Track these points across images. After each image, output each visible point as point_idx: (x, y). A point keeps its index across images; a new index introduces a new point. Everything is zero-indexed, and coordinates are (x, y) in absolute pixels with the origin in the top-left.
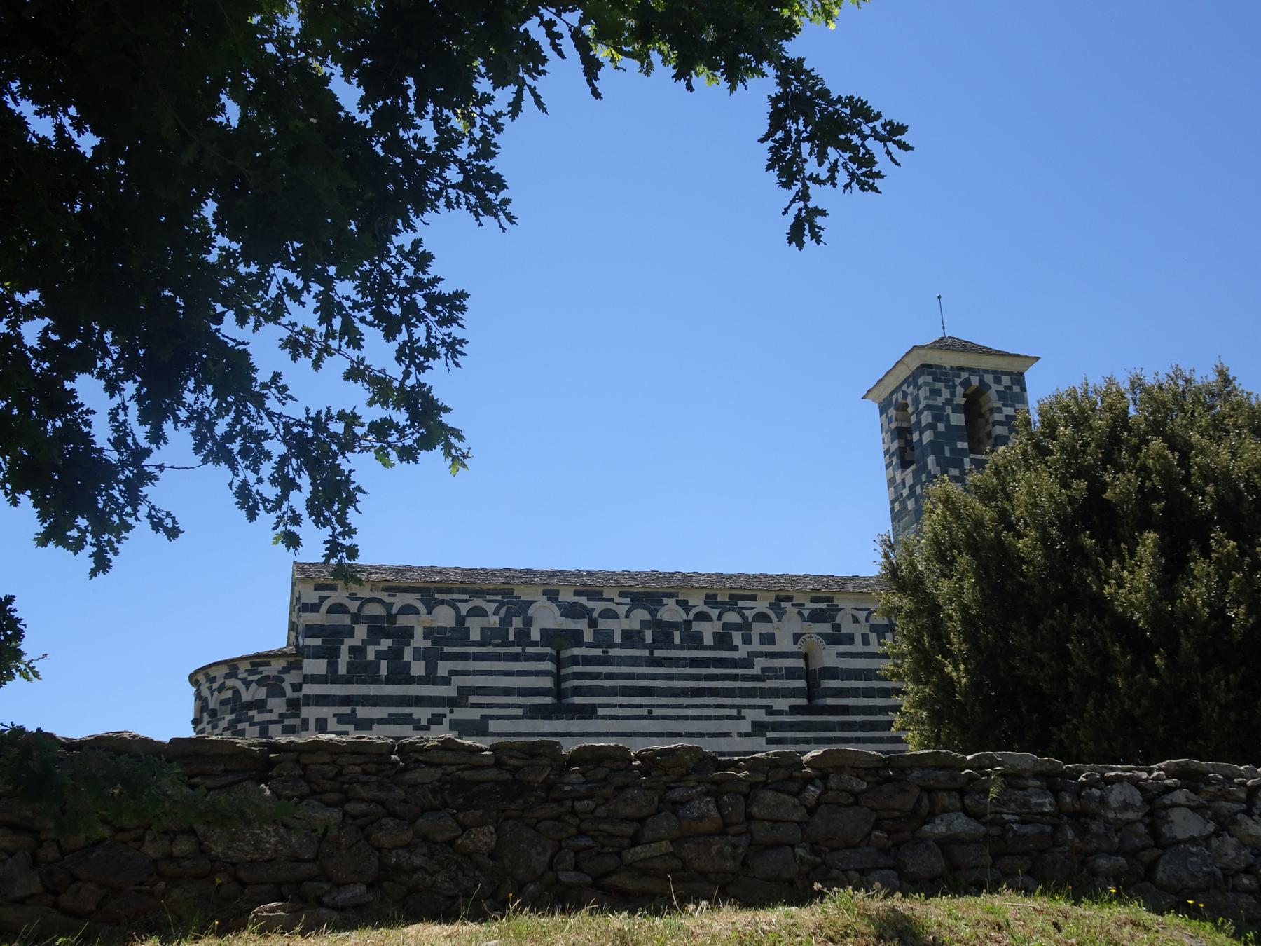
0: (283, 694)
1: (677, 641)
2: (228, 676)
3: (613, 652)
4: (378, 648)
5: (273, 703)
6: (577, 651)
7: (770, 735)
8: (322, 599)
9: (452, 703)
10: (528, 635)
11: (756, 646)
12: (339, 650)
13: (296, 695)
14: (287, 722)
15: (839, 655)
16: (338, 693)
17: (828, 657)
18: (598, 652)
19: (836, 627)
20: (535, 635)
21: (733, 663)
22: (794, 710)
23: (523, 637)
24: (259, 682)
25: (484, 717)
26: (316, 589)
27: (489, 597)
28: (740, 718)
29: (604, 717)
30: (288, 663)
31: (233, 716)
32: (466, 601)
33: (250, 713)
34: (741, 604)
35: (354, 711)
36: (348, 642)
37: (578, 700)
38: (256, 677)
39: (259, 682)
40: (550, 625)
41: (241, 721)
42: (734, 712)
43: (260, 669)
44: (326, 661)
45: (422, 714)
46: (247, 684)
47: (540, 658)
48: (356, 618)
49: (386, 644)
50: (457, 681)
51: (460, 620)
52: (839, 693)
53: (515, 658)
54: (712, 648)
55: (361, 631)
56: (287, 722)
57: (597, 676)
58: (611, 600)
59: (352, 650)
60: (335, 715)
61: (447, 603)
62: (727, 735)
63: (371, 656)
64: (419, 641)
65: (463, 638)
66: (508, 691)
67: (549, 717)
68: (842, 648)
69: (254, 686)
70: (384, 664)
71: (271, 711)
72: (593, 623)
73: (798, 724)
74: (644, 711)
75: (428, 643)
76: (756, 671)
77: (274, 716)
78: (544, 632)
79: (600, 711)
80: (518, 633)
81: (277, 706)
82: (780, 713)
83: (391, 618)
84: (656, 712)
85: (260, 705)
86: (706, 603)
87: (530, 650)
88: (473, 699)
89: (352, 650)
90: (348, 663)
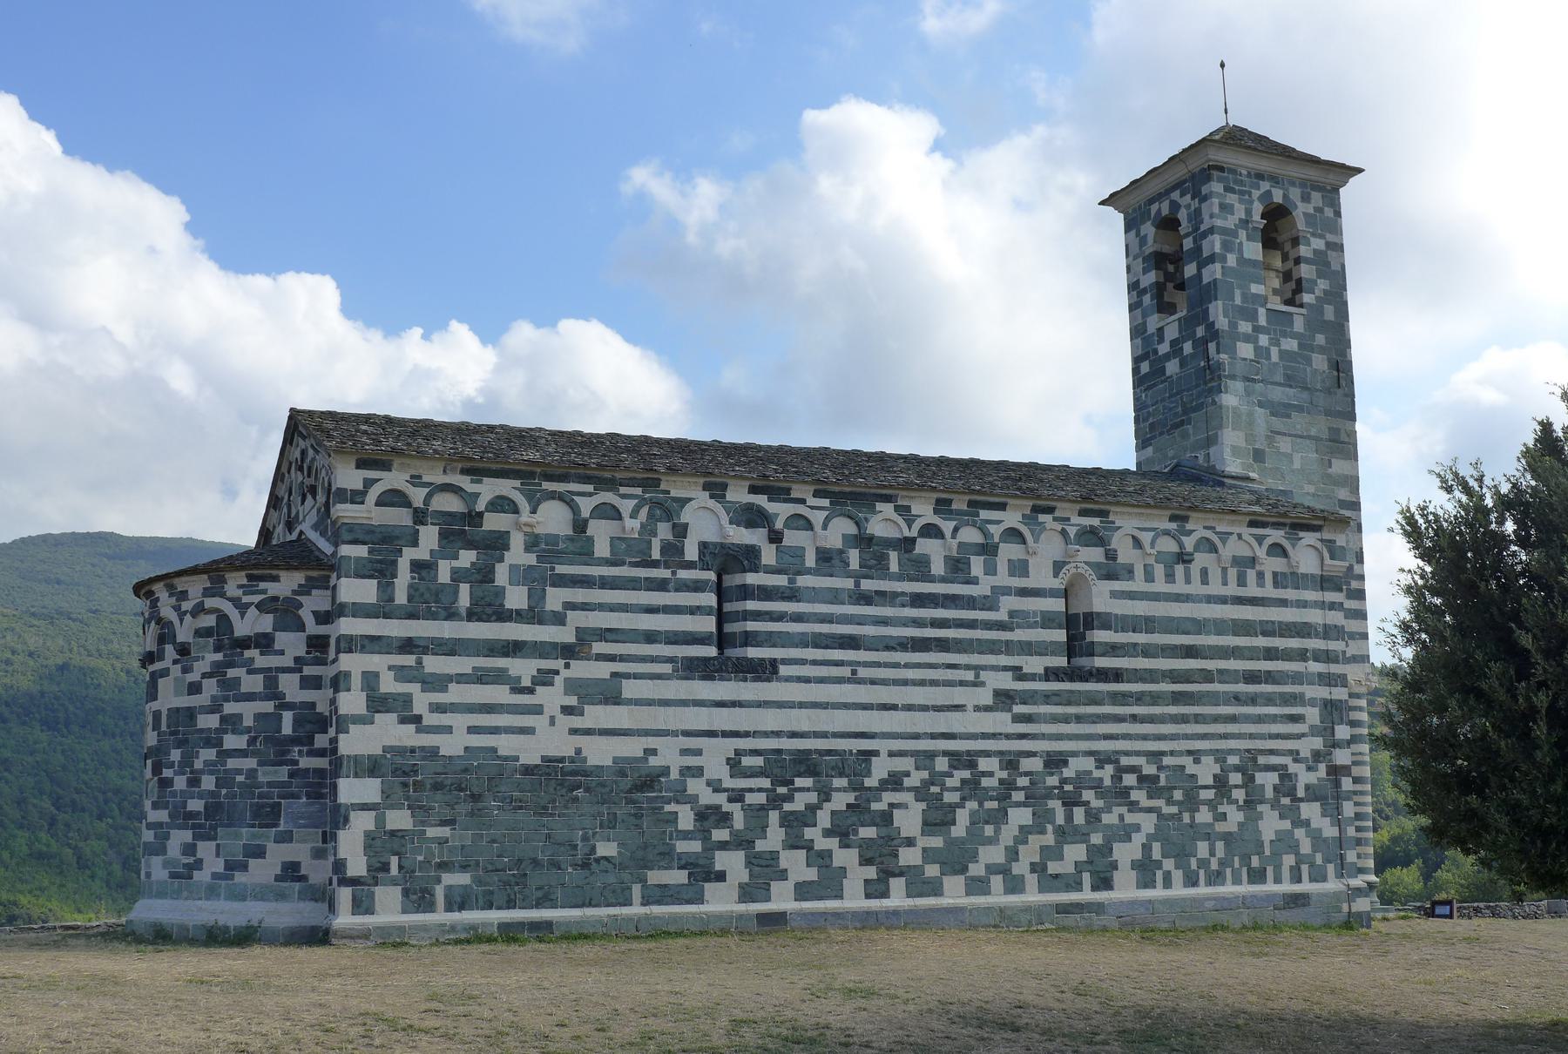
0: (301, 627)
1: (894, 567)
2: (207, 593)
3: (804, 581)
4: (455, 564)
5: (283, 639)
6: (751, 579)
7: (1019, 709)
8: (369, 483)
9: (568, 652)
10: (682, 552)
11: (1003, 578)
12: (394, 563)
13: (322, 630)
14: (308, 671)
15: (1115, 595)
16: (394, 633)
17: (1101, 597)
18: (781, 581)
19: (1111, 556)
20: (691, 553)
21: (970, 603)
22: (1051, 674)
23: (673, 552)
24: (259, 606)
25: (614, 675)
26: (358, 467)
27: (623, 490)
28: (977, 684)
29: (788, 679)
30: (308, 579)
31: (219, 657)
32: (590, 495)
33: (248, 654)
34: (984, 514)
35: (419, 662)
36: (409, 554)
37: (753, 653)
38: (257, 598)
39: (259, 606)
40: (711, 537)
41: (231, 665)
42: (969, 676)
43: (262, 585)
44: (375, 582)
45: (524, 668)
46: (242, 608)
47: (697, 586)
48: (420, 517)
49: (467, 558)
50: (576, 619)
51: (580, 526)
52: (1113, 650)
53: (662, 585)
54: (943, 580)
55: (429, 536)
56: (308, 671)
57: (780, 617)
58: (803, 501)
60: (390, 668)
61: (560, 497)
62: (958, 708)
63: (444, 576)
64: (517, 554)
65: (585, 553)
66: (650, 637)
67: (710, 678)
68: (1117, 585)
69: (253, 611)
70: (464, 588)
71: (282, 653)
72: (775, 538)
73: (1056, 694)
74: (845, 672)
75: (531, 559)
76: (1001, 615)
77: (286, 661)
78: (703, 546)
79: (784, 670)
80: (667, 548)
81: (292, 645)
82: (1032, 677)
83: (474, 518)
84: (863, 673)
85: (264, 642)
86: (936, 512)
87: (683, 574)
88: (599, 647)
89: (417, 566)
90: (411, 586)
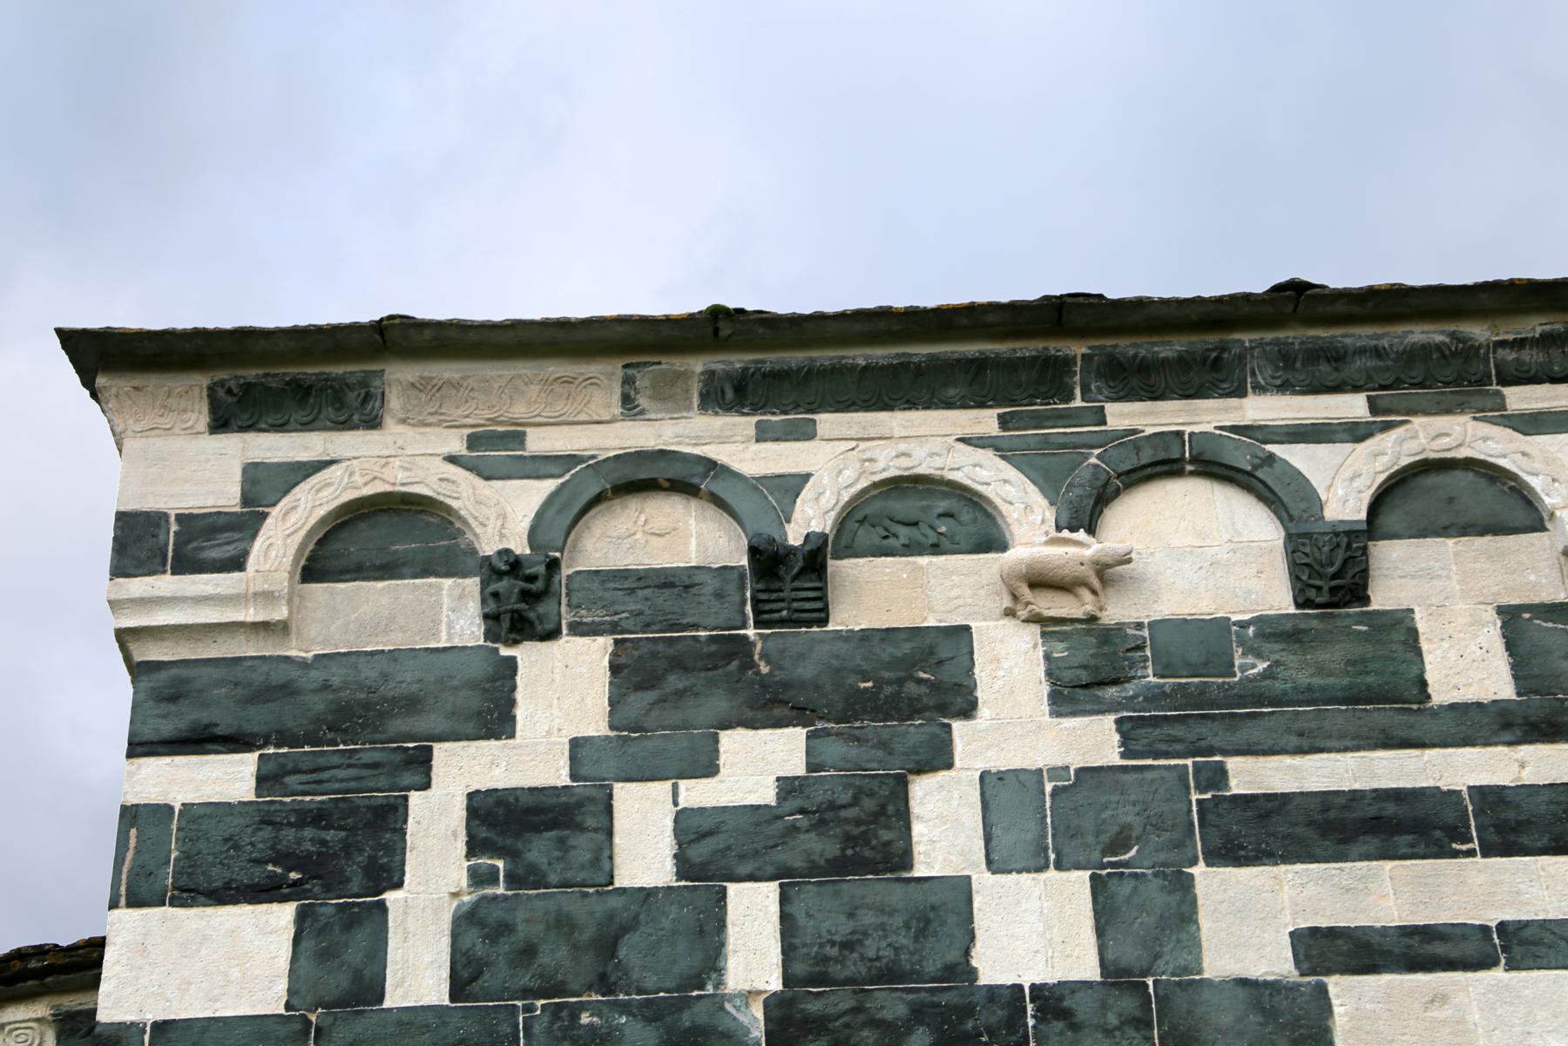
4: (697, 793)
8: (265, 487)
12: (391, 818)
26: (221, 423)
27: (1520, 398)
32: (1356, 433)
36: (463, 769)
48: (524, 599)
49: (757, 764)
51: (1331, 571)
55: (566, 688)
59: (497, 820)
61: (1210, 464)
63: (643, 841)
64: (1017, 721)
65: (1388, 696)
70: (753, 911)
75: (1094, 740)
83: (788, 577)
89: (497, 820)
90: (465, 921)
